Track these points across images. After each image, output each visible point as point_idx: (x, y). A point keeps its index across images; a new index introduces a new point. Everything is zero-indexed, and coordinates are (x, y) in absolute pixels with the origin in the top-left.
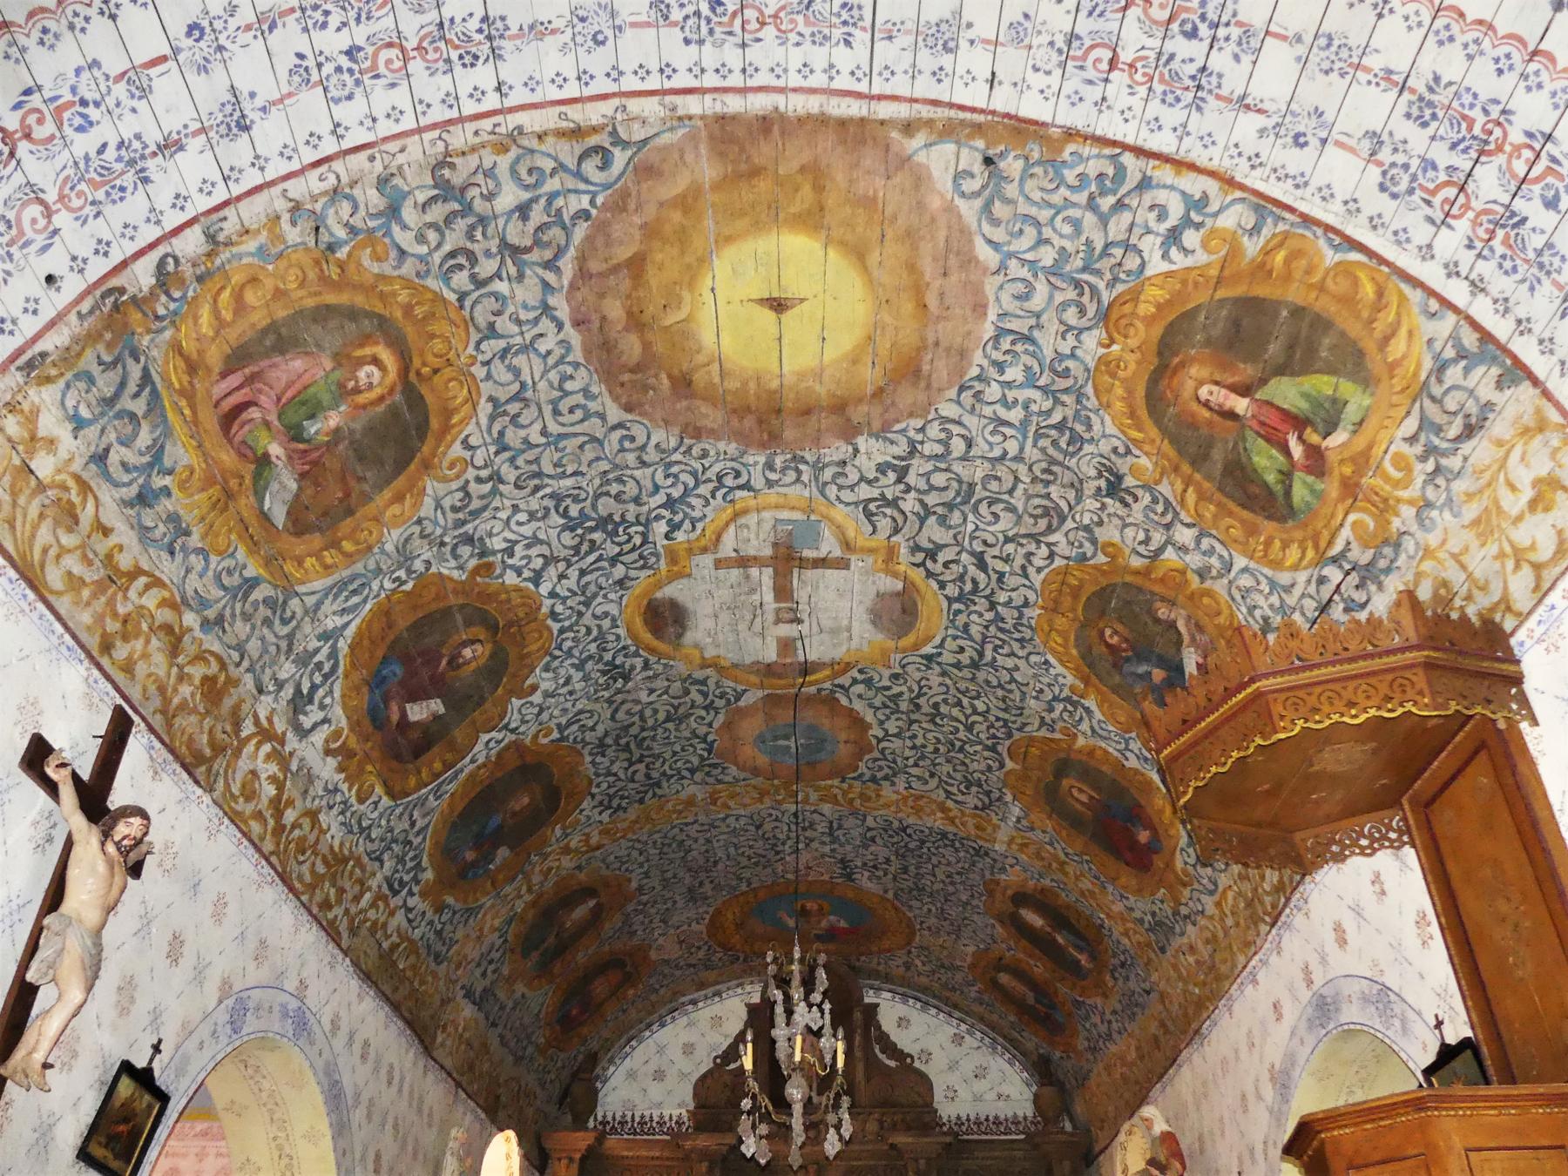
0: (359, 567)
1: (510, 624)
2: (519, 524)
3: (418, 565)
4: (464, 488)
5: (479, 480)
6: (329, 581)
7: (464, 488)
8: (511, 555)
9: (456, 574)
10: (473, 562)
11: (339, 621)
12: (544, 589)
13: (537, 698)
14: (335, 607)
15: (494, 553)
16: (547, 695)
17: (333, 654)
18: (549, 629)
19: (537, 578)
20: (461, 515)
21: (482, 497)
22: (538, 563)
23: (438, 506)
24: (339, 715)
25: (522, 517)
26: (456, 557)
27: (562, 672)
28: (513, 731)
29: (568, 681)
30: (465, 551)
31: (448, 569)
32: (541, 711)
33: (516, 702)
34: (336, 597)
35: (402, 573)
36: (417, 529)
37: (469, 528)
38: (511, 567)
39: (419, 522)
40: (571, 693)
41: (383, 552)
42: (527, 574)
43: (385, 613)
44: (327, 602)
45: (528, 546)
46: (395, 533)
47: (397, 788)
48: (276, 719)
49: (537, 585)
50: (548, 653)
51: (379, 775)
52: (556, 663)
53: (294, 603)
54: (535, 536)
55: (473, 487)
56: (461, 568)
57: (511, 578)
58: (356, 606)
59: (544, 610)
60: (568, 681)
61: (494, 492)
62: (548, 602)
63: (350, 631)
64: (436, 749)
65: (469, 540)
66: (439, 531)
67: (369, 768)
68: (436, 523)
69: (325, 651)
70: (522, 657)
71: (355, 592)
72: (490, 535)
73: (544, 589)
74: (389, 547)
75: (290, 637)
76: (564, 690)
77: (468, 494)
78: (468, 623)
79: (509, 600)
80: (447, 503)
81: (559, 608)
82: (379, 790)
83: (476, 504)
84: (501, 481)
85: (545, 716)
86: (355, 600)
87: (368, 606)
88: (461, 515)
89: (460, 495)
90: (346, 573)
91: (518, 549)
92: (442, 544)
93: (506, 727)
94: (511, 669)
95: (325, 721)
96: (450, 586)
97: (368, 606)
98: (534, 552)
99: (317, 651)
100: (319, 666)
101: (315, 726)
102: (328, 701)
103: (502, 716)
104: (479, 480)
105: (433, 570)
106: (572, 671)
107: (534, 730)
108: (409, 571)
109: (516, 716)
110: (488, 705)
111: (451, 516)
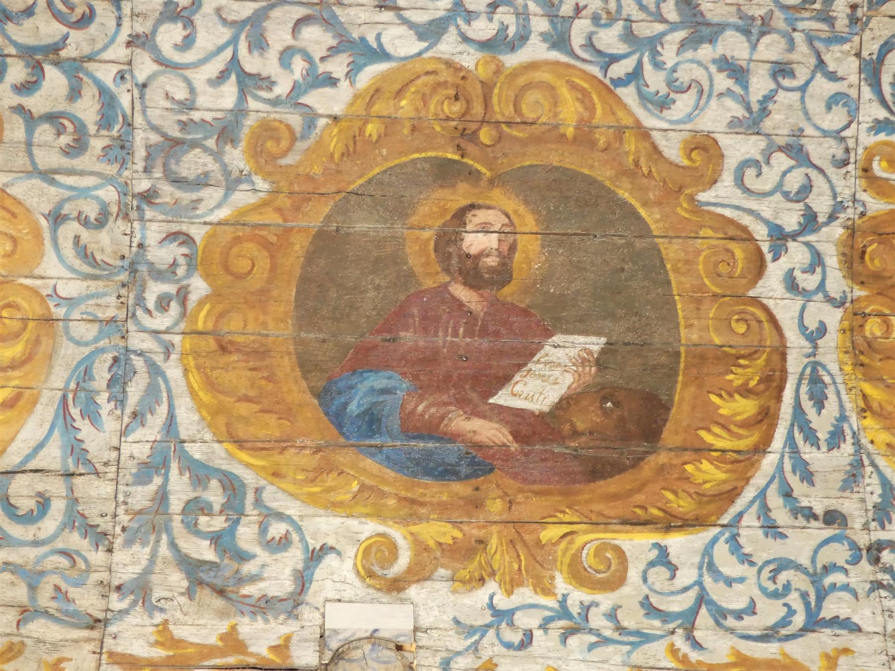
0: (69, 354)
1: (465, 136)
2: (187, 43)
3: (163, 254)
4: (30, 119)
5: (27, 88)
6: (44, 412)
7: (30, 119)
8: (268, 83)
9: (243, 198)
10: (237, 158)
11: (151, 430)
12: (402, 43)
13: (738, 148)
14: (111, 425)
15: (240, 111)
16: (752, 122)
17: (200, 473)
18: (533, 66)
19: (369, 52)
20: (97, 145)
21: (75, 93)
22: (316, 38)
23: (48, 176)
24: (324, 526)
25: (169, 36)
26: (202, 182)
27: (683, 76)
28: (810, 222)
29: (738, 72)
30: (193, 163)
31: (216, 208)
32: (796, 151)
33: (722, 194)
34: (92, 415)
35: (154, 290)
36: (71, 229)
37: (141, 138)
38: (296, 89)
39: (57, 218)
40: (781, 70)
41: (71, 301)
42: (338, 67)
43: (217, 347)
44: (85, 429)
45: (259, 44)
46: (50, 266)
47: (683, 505)
48: (179, 632)
49: (382, 55)
50: (608, 90)
51: (599, 523)
52: (655, 81)
53: (22, 491)
54: (238, 25)
55: (36, 103)
56: (232, 183)
57: (329, 102)
58: (152, 391)
59: (470, 59)
60: (738, 72)
61: (75, 70)
62: (447, 45)
63: (188, 419)
64: (683, 395)
65: (174, 146)
66: (109, 194)
67: (550, 533)
68: (84, 193)
69: (180, 488)
70: (584, 137)
71: (118, 384)
72: (188, 105)
73: (402, 43)
74: (71, 288)
75: (76, 520)
76: (760, 84)
77: (52, 118)
78: (401, 210)
79: (391, 123)
80: (48, 158)
81: (483, 29)
82: (638, 544)
83: (87, 110)
84: (53, 50)
85: (821, 151)
86: (135, 391)
87: (173, 371)
88: (97, 145)
89: (44, 132)
90: (59, 377)
91: (251, 63)
92: (148, 197)
93: (780, 238)
94: (603, 174)
95: (315, 556)
96: (271, 217)
97: (173, 371)
98: (279, 35)
99: (162, 497)
100: (196, 507)
101: (303, 580)
102: (277, 529)
103: (745, 236)
104: (27, 88)
105: (198, 233)
106: (705, 52)
107: (847, 184)
108: (166, 273)
109: (766, 208)
110: (672, 251)
111: (83, 162)
